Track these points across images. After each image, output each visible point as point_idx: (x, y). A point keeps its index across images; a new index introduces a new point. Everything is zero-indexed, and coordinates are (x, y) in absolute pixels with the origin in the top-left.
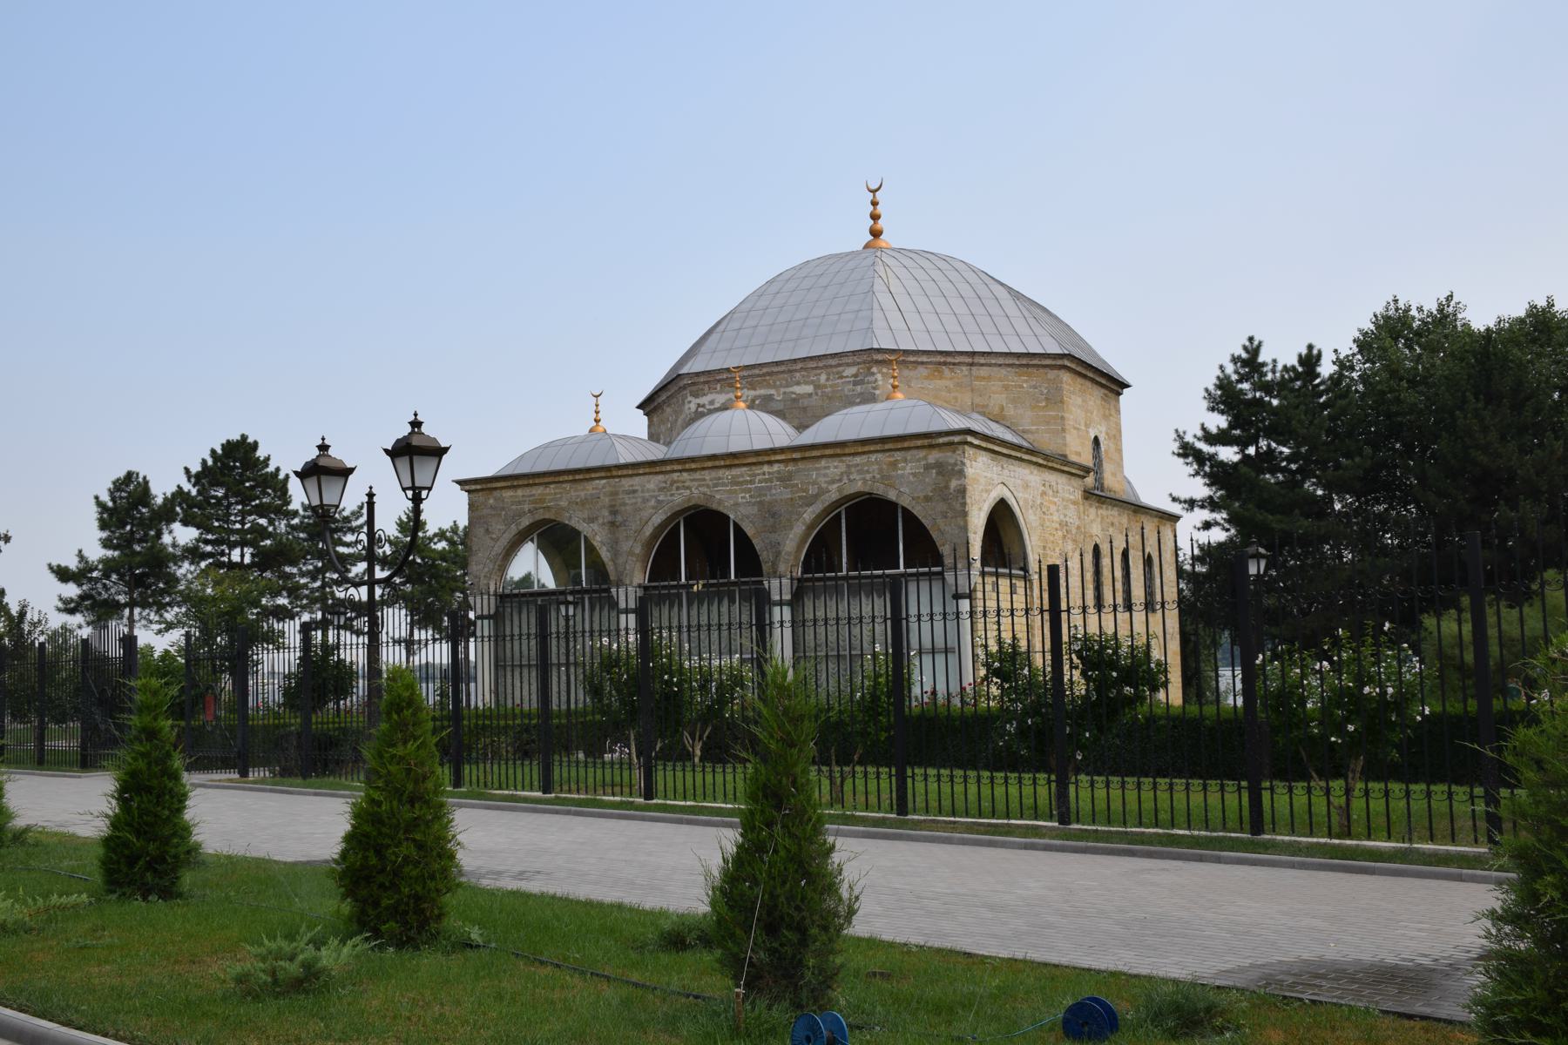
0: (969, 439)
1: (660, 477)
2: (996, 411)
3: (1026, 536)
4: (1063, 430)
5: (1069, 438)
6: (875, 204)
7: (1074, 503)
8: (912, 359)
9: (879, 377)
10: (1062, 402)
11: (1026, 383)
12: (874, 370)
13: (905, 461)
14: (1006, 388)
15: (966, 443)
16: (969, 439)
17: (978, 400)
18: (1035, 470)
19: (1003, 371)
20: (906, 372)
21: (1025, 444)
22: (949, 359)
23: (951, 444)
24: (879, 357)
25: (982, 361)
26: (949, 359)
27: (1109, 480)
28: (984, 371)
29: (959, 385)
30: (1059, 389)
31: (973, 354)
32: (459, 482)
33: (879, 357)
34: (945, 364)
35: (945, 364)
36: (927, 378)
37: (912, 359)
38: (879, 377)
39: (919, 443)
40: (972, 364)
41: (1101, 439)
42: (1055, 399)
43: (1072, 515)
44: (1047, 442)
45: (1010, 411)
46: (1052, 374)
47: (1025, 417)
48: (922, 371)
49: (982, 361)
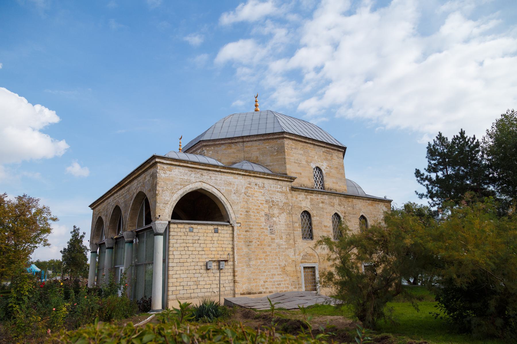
0: (157, 160)
1: (112, 197)
2: (255, 158)
3: (228, 206)
4: (285, 163)
5: (288, 166)
6: (256, 101)
7: (281, 192)
8: (217, 143)
9: (205, 151)
10: (284, 152)
11: (267, 146)
12: (204, 149)
13: (147, 175)
14: (259, 149)
15: (156, 162)
16: (157, 160)
17: (246, 155)
18: (240, 177)
19: (258, 143)
20: (216, 148)
21: (267, 171)
22: (233, 141)
23: (153, 164)
24: (205, 144)
25: (247, 140)
26: (233, 141)
27: (329, 183)
28: (249, 144)
29: (239, 150)
30: (283, 147)
31: (242, 137)
32: (90, 206)
33: (205, 144)
34: (232, 143)
35: (232, 143)
36: (225, 149)
37: (217, 143)
38: (205, 151)
39: (148, 166)
40: (243, 142)
41: (323, 168)
42: (281, 151)
43: (279, 198)
44: (278, 169)
45: (261, 158)
46: (279, 141)
47: (268, 160)
48: (223, 147)
49: (247, 140)
